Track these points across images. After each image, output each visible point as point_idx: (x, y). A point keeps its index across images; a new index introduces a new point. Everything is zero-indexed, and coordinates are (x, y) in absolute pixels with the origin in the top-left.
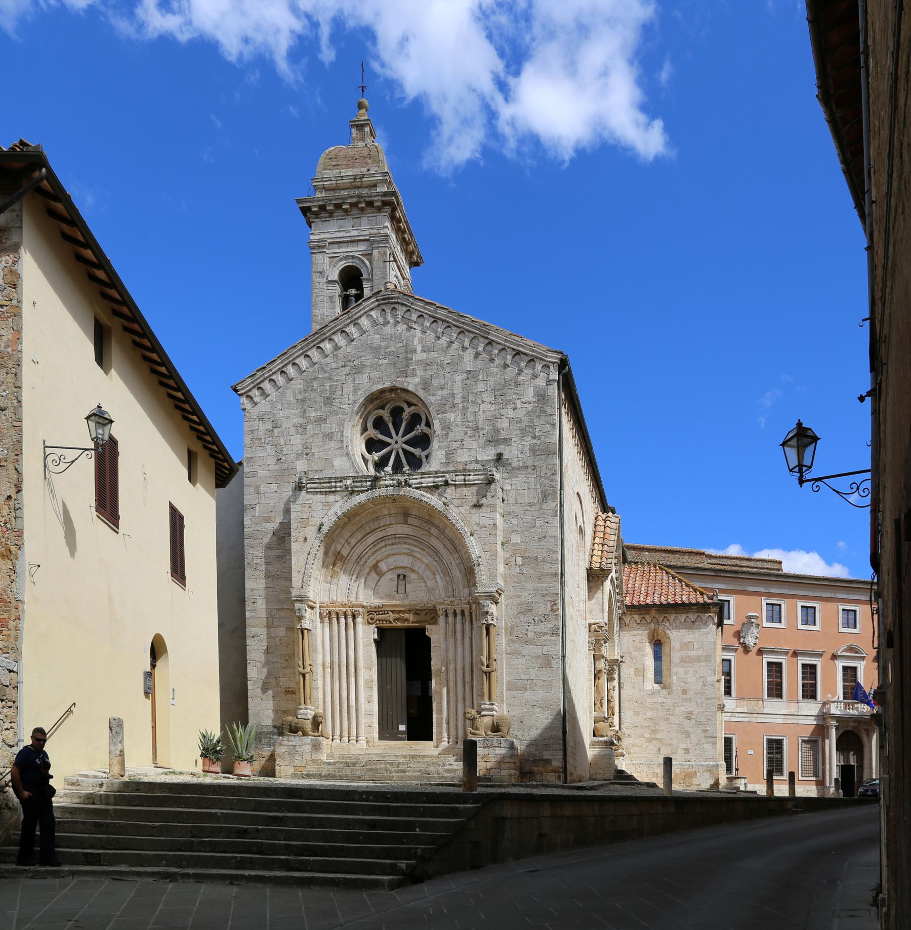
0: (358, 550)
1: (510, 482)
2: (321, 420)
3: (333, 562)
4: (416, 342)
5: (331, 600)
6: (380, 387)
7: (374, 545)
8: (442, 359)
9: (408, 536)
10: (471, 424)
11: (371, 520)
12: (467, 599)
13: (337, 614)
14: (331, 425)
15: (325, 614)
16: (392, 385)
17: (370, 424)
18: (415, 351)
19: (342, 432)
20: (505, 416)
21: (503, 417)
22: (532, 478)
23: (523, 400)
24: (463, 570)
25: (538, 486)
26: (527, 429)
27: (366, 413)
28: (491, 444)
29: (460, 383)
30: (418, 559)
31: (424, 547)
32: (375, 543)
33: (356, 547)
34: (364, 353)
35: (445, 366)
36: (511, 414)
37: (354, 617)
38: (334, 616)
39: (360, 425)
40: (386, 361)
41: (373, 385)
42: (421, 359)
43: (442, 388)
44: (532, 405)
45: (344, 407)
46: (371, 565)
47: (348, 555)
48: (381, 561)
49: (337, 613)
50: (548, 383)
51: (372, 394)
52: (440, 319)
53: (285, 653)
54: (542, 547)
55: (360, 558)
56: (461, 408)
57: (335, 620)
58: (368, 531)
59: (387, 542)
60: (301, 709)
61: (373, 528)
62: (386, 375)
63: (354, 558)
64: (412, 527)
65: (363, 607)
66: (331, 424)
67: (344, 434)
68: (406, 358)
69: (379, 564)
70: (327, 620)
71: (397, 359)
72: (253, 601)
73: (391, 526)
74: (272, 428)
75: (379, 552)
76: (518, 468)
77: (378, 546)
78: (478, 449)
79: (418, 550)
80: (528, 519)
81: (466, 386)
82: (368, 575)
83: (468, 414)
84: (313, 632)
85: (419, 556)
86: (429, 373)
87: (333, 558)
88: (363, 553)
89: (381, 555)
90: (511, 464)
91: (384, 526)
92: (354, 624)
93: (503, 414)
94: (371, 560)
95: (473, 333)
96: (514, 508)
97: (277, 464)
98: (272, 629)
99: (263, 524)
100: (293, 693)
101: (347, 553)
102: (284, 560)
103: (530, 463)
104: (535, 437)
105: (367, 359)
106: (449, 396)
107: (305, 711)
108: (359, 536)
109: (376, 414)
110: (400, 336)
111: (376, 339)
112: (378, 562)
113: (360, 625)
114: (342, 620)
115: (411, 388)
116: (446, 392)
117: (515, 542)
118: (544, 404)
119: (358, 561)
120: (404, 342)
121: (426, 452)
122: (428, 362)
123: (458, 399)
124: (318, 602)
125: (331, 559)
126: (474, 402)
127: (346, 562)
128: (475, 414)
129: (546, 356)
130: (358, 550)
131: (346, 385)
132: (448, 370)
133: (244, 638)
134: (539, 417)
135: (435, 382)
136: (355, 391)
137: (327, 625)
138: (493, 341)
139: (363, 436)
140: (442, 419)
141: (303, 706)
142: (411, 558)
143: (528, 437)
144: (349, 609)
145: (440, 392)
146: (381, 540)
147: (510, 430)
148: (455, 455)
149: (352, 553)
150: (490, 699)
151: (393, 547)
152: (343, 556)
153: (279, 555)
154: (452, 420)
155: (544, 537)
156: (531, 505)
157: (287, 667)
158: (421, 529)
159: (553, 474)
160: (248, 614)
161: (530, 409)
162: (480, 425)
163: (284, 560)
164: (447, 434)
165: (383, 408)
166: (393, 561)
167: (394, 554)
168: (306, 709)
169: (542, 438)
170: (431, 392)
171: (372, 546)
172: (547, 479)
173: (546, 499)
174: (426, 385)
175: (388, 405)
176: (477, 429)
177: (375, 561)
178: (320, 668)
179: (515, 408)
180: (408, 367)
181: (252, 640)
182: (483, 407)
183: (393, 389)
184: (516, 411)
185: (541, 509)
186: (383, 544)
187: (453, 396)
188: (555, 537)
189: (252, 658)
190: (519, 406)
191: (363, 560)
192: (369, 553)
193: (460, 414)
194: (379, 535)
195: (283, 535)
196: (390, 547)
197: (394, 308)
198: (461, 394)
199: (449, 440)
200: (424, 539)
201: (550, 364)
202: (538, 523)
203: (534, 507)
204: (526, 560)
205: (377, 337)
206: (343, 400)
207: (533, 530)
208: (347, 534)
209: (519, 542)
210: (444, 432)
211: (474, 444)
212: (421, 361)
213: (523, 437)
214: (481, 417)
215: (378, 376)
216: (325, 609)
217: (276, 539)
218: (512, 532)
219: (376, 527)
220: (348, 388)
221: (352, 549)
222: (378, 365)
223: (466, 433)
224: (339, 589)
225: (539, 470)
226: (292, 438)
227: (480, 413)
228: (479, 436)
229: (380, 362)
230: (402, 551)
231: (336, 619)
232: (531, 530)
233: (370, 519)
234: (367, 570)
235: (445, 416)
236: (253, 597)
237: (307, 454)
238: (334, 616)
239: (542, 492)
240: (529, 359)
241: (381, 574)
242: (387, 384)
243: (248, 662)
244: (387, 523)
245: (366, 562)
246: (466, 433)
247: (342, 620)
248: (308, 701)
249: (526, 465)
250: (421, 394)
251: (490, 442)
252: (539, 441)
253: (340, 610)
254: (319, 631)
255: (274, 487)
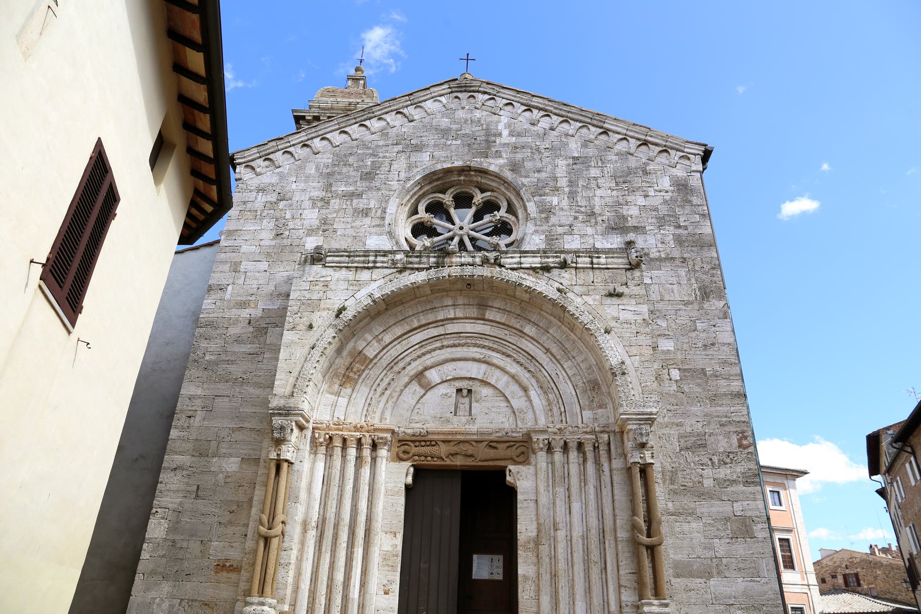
0: (394, 352)
1: (649, 275)
2: (351, 196)
3: (347, 364)
4: (501, 127)
5: (335, 419)
6: (447, 165)
7: (422, 346)
8: (537, 143)
9: (481, 336)
10: (583, 209)
11: (423, 311)
12: (591, 425)
13: (344, 440)
14: (371, 201)
15: (321, 440)
16: (465, 165)
17: (422, 207)
18: (500, 135)
19: (385, 209)
20: (633, 203)
21: (629, 204)
22: (682, 272)
23: (656, 188)
24: (580, 384)
25: (693, 281)
26: (667, 218)
27: (420, 193)
28: (614, 231)
29: (564, 168)
30: (498, 367)
31: (509, 352)
32: (423, 343)
33: (390, 347)
34: (426, 134)
35: (543, 151)
36: (641, 201)
37: (374, 446)
38: (338, 443)
39: (410, 204)
40: (459, 142)
41: (436, 163)
42: (507, 142)
43: (539, 171)
44: (670, 194)
45: (390, 183)
46: (412, 373)
47: (376, 356)
48: (431, 367)
49: (344, 440)
50: (689, 174)
51: (434, 173)
52: (537, 108)
53: (230, 498)
54: (710, 357)
55: (395, 361)
56: (567, 192)
57: (338, 452)
58: (416, 324)
59: (445, 343)
60: (252, 604)
61: (424, 322)
62: (456, 155)
63: (385, 361)
64: (491, 323)
65: (393, 432)
66: (369, 199)
67: (388, 211)
68: (487, 141)
69: (427, 374)
70: (323, 449)
71: (473, 141)
72: (190, 413)
73: (455, 321)
74: (275, 200)
75: (428, 356)
76: (660, 259)
77: (429, 348)
78: (596, 236)
79: (499, 355)
80: (683, 319)
81: (573, 171)
82: (405, 387)
83: (579, 199)
84: (295, 467)
85: (501, 364)
86: (519, 156)
87: (349, 360)
88: (399, 358)
89: (432, 360)
90: (647, 255)
91: (442, 320)
92: (374, 459)
93: (631, 200)
94: (414, 364)
95: (580, 121)
96: (660, 306)
97: (274, 239)
98: (216, 459)
99: (234, 310)
100: (236, 569)
101: (376, 353)
102: (260, 359)
103: (676, 254)
104: (679, 227)
105: (430, 139)
106: (549, 179)
107: (259, 608)
108: (398, 331)
109: (433, 198)
110: (479, 121)
111: (445, 122)
112: (426, 369)
113: (385, 460)
114: (352, 452)
115: (492, 168)
116: (543, 175)
117: (665, 349)
118: (687, 194)
119: (390, 366)
120: (484, 126)
121: (509, 240)
122: (517, 145)
123: (563, 182)
124: (311, 421)
125: (342, 362)
126: (586, 187)
127: (370, 366)
128: (589, 199)
129: (685, 147)
130: (394, 352)
131: (396, 162)
132: (547, 154)
133: (157, 469)
134: (682, 207)
135: (528, 165)
136: (410, 167)
137: (321, 457)
138: (610, 130)
139: (410, 220)
140: (540, 202)
141: (255, 599)
142: (484, 367)
143: (670, 225)
144: (367, 435)
145: (536, 175)
146: (435, 339)
147: (641, 218)
148: (561, 241)
149: (382, 354)
150: (657, 594)
151: (454, 349)
152: (366, 357)
153: (252, 351)
154: (555, 202)
155: (713, 344)
156: (687, 303)
157: (230, 523)
158: (506, 327)
159: (713, 268)
160: (174, 433)
161: (668, 198)
162: (597, 210)
163: (260, 359)
164: (547, 219)
165: (443, 192)
166: (450, 370)
167: (454, 360)
168: (263, 604)
169: (690, 229)
170: (523, 173)
171: (417, 346)
172: (706, 273)
173: (708, 297)
174: (515, 167)
175: (452, 190)
176: (593, 214)
177: (421, 368)
178: (298, 529)
179: (646, 196)
180: (489, 148)
181: (172, 474)
182: (599, 192)
183: (464, 170)
184: (647, 198)
185: (702, 308)
186: (438, 344)
187: (555, 179)
188: (729, 344)
189: (163, 504)
190: (651, 193)
191: (401, 365)
192: (414, 355)
193: (566, 198)
194: (434, 332)
195: (266, 326)
196: (449, 350)
197: (473, 96)
198: (567, 179)
199: (550, 224)
200: (510, 340)
201: (690, 156)
202: (699, 326)
203: (690, 306)
204: (688, 374)
205: (447, 120)
206: (389, 176)
207: (694, 334)
208: (377, 330)
209: (672, 349)
210: (543, 216)
211: (590, 231)
212: (508, 144)
213: (662, 226)
214: (597, 202)
215: (446, 155)
216: (323, 433)
217: (251, 329)
218: (659, 335)
219: (430, 321)
220: (400, 164)
221: (383, 349)
222: (445, 145)
223: (576, 218)
224: (351, 404)
225: (691, 263)
226: (306, 212)
227: (596, 198)
228: (596, 223)
229: (449, 142)
230: (471, 355)
231: (339, 449)
232: (690, 335)
233: (420, 310)
234: (406, 379)
235: (543, 199)
236: (190, 408)
237: (324, 231)
238: (338, 443)
239: (700, 289)
240: (661, 149)
241: (428, 387)
242: (458, 164)
243: (154, 510)
244: (449, 317)
245: (404, 368)
246: (576, 218)
247: (352, 452)
248: (268, 589)
249: (670, 256)
250: (508, 175)
251: (613, 229)
252: (686, 232)
253: (352, 436)
254: (306, 466)
255: (264, 265)
